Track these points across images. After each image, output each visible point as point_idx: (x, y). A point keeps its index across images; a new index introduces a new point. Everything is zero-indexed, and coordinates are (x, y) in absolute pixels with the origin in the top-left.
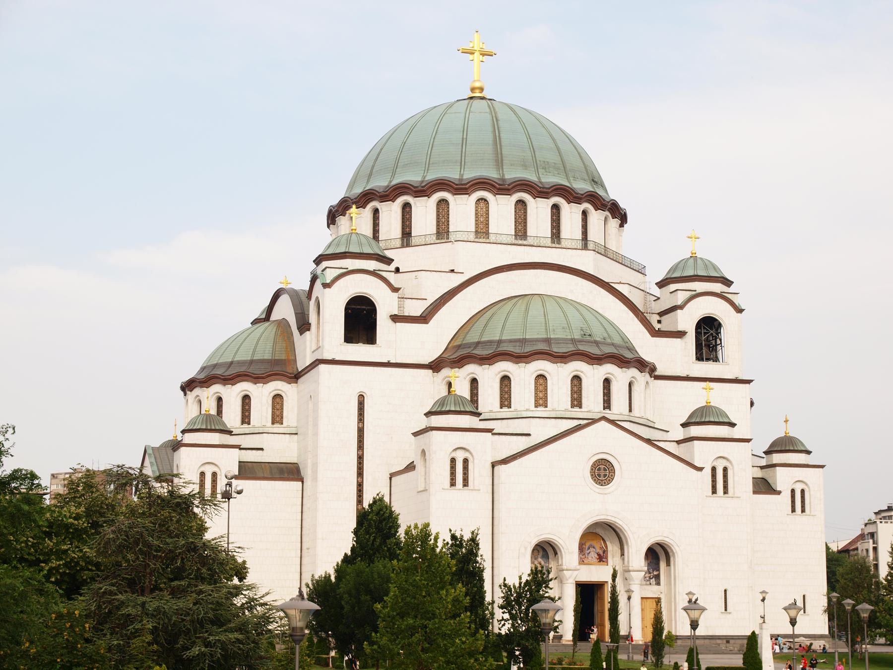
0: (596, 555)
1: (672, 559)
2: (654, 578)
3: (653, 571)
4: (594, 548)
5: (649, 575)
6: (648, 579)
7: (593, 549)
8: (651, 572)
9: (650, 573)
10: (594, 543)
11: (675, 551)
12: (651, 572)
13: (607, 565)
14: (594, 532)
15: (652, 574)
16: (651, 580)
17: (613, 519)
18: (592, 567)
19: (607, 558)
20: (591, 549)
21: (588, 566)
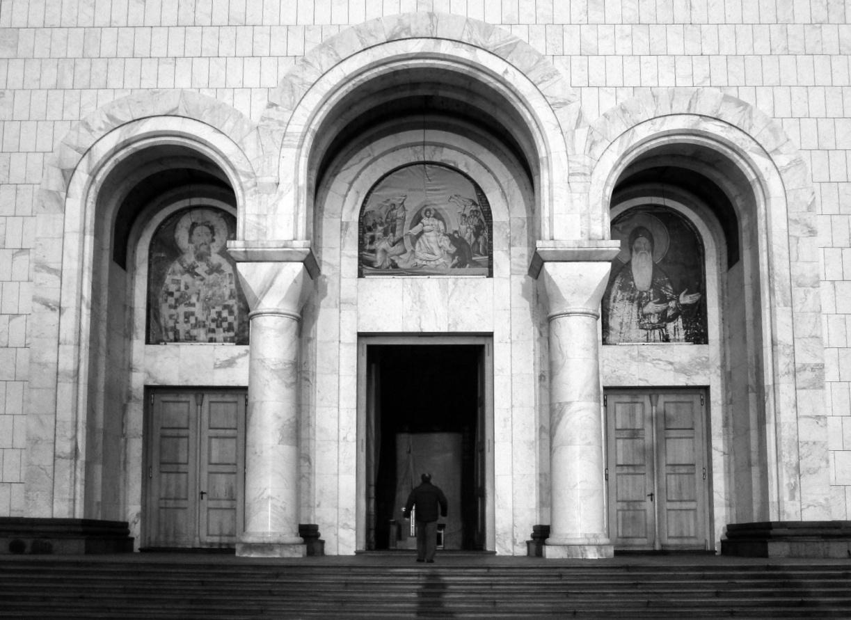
0: (446, 243)
1: (744, 223)
2: (680, 320)
3: (677, 292)
4: (438, 216)
5: (661, 307)
6: (654, 320)
7: (436, 222)
8: (669, 294)
9: (663, 299)
10: (439, 200)
11: (751, 176)
12: (669, 294)
13: (491, 275)
14: (437, 159)
15: (672, 304)
16: (670, 326)
17: (464, 53)
18: (430, 285)
19: (489, 252)
20: (425, 221)
21: (408, 280)
